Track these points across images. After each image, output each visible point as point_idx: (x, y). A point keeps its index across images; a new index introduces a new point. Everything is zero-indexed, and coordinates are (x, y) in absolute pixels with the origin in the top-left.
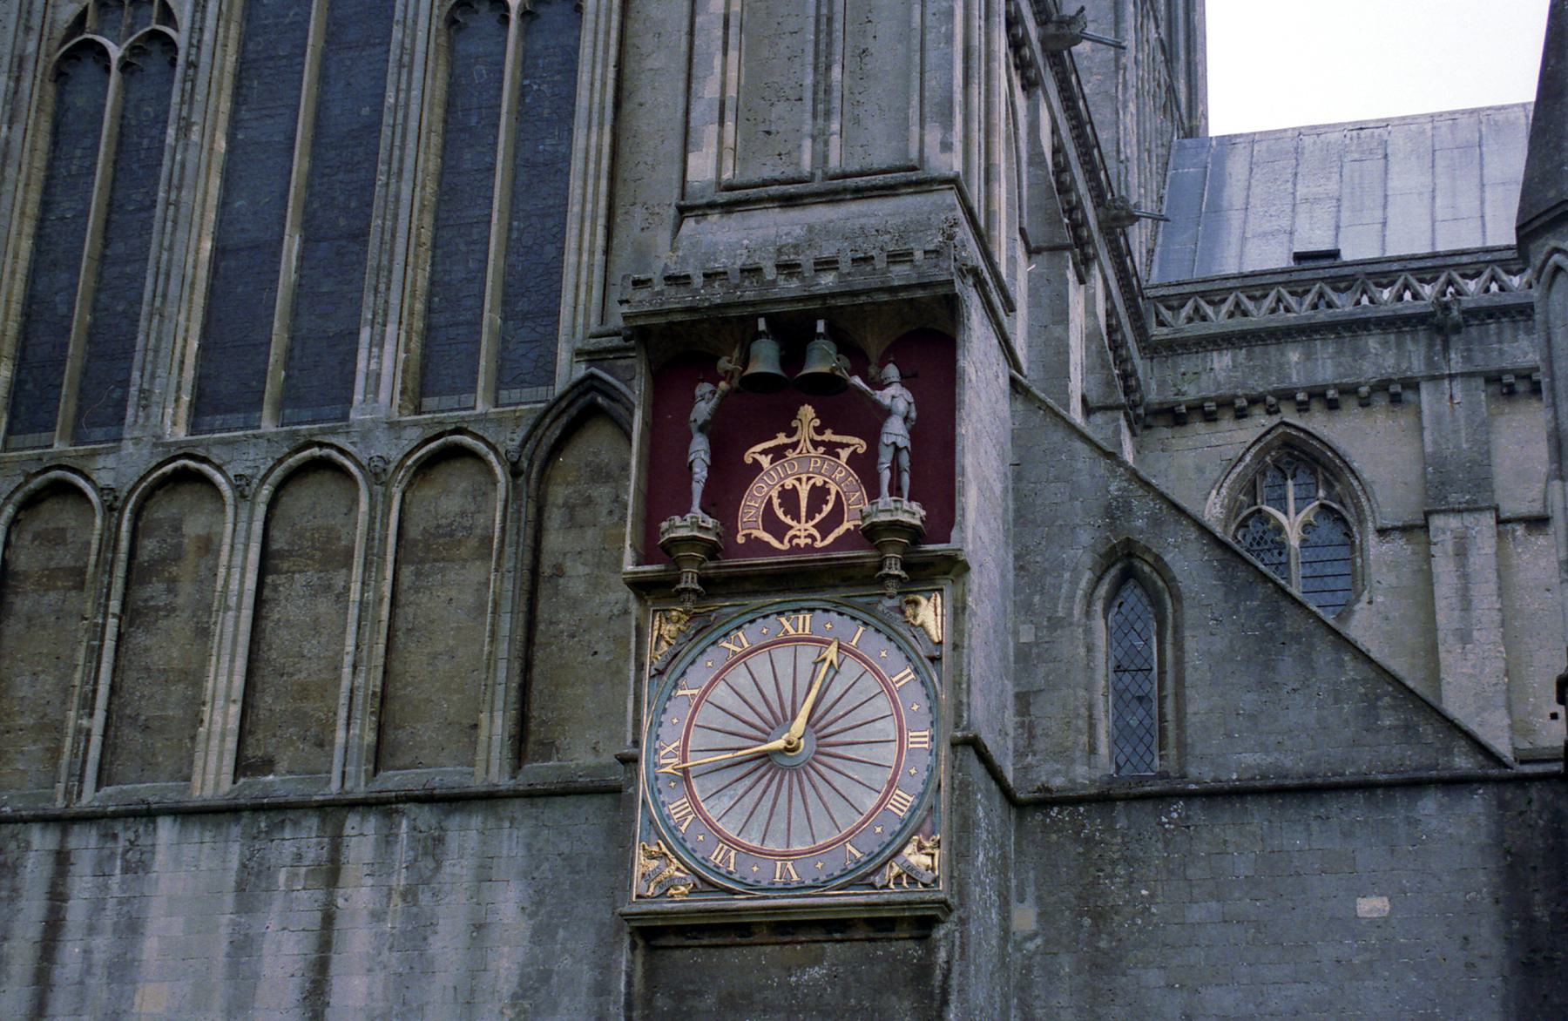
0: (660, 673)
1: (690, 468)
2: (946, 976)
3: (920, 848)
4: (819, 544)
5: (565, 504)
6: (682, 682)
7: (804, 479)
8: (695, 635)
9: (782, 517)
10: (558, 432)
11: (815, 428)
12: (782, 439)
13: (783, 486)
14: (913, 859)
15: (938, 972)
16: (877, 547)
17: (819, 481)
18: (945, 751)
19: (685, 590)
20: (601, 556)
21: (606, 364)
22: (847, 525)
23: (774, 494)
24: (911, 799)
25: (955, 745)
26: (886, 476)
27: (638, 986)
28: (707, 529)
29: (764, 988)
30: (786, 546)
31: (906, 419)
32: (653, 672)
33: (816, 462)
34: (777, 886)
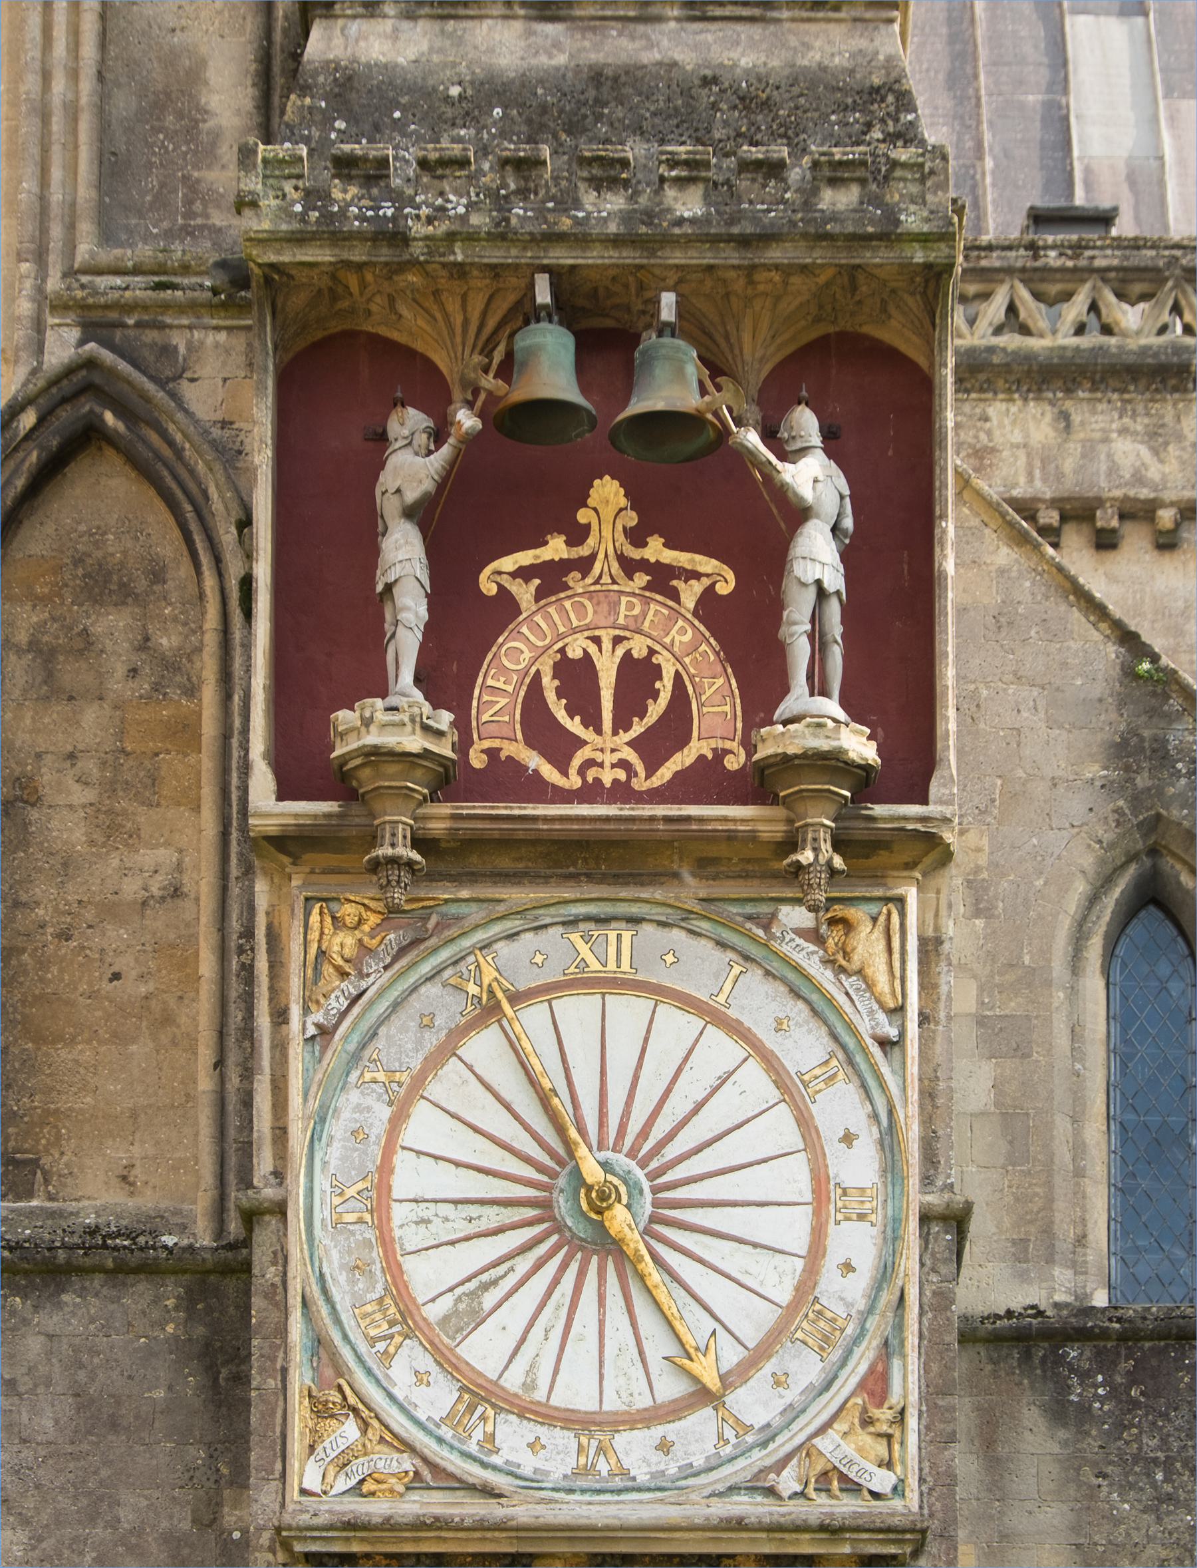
4: (641, 783)
7: (607, 644)
9: (561, 715)
21: (118, 334)
30: (575, 782)
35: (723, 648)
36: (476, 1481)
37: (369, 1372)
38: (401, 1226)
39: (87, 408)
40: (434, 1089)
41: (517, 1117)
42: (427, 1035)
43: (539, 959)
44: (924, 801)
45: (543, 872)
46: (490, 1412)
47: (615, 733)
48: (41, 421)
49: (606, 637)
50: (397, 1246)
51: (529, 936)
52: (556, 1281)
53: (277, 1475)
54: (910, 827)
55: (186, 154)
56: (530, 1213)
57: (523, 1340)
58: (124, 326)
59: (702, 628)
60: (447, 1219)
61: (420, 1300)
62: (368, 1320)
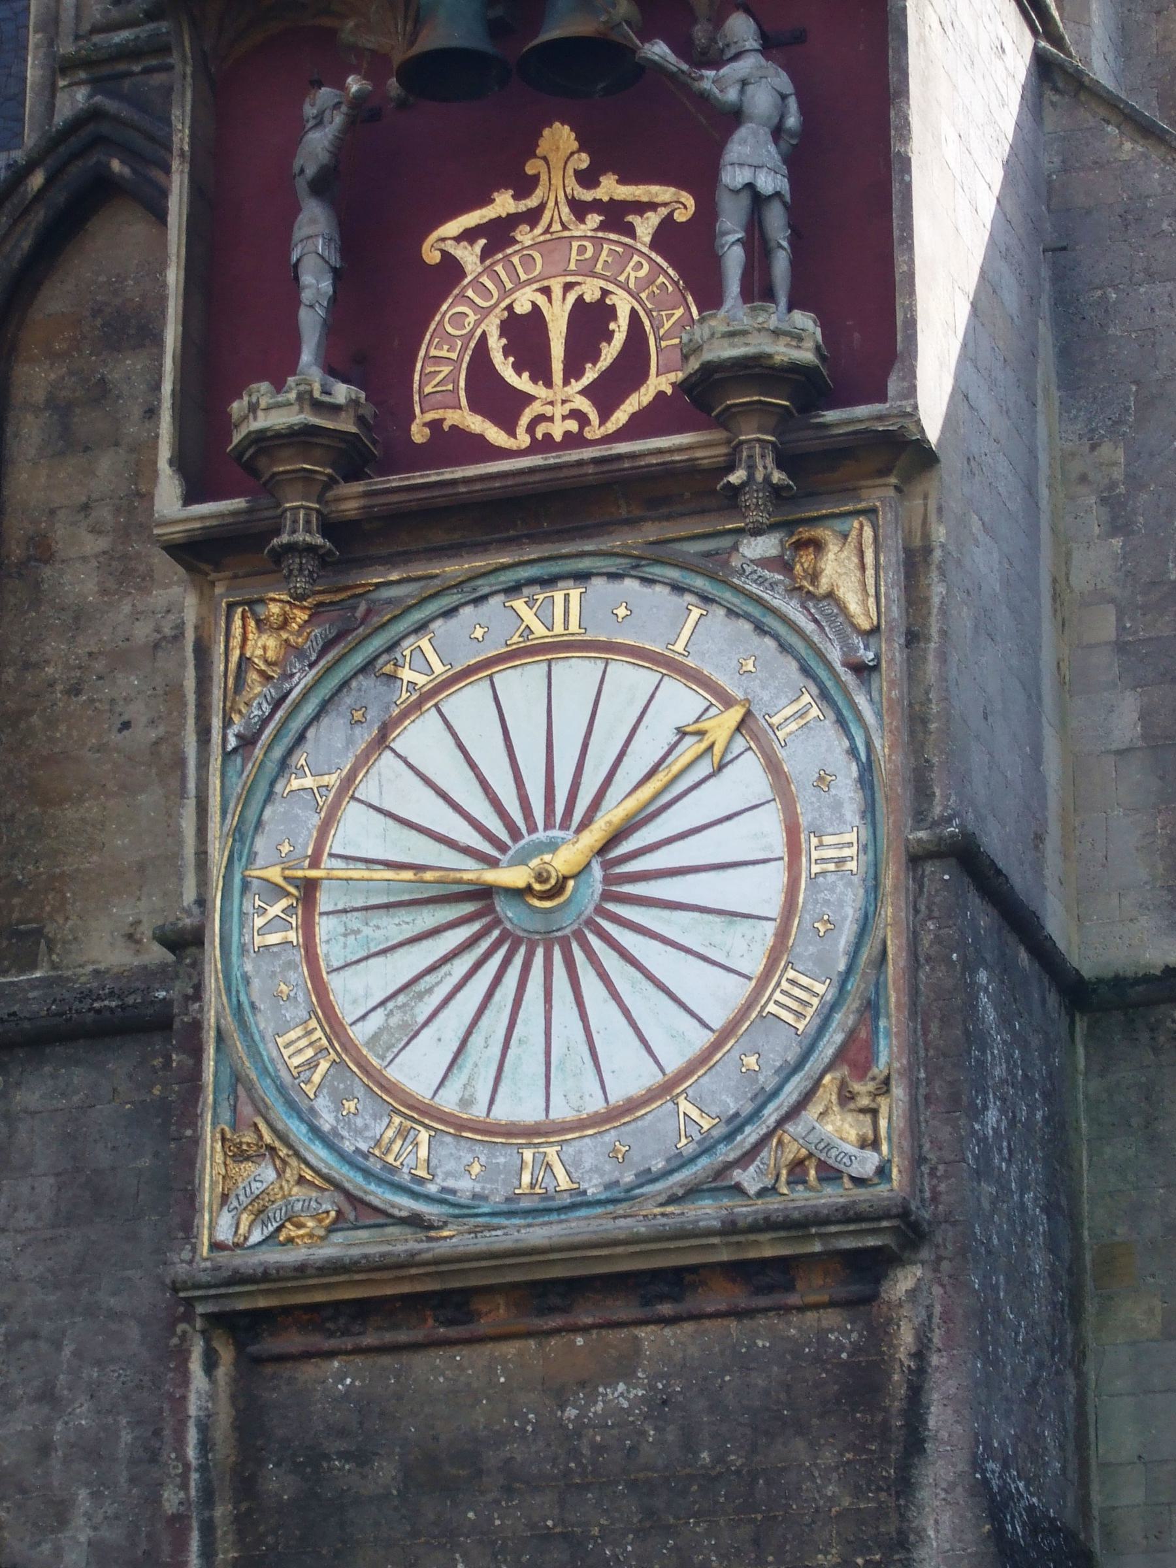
0: (247, 741)
3: (846, 1097)
4: (594, 431)
5: (51, 402)
6: (300, 759)
7: (557, 291)
8: (322, 653)
10: (26, 244)
13: (510, 308)
14: (828, 1128)
15: (896, 1377)
17: (590, 291)
19: (291, 548)
21: (126, 84)
22: (658, 384)
23: (492, 327)
24: (820, 988)
25: (915, 859)
26: (734, 259)
27: (225, 1449)
28: (335, 409)
30: (524, 440)
31: (777, 132)
32: (232, 742)
33: (582, 250)
34: (525, 1204)
35: (681, 276)
36: (404, 1214)
37: (291, 1105)
38: (328, 942)
39: (95, 159)
40: (367, 789)
42: (358, 730)
43: (479, 633)
44: (882, 397)
46: (424, 1136)
47: (566, 382)
48: (49, 181)
50: (322, 964)
51: (467, 611)
56: (468, 908)
58: (131, 74)
59: (659, 260)
61: (348, 1020)
62: (292, 1049)
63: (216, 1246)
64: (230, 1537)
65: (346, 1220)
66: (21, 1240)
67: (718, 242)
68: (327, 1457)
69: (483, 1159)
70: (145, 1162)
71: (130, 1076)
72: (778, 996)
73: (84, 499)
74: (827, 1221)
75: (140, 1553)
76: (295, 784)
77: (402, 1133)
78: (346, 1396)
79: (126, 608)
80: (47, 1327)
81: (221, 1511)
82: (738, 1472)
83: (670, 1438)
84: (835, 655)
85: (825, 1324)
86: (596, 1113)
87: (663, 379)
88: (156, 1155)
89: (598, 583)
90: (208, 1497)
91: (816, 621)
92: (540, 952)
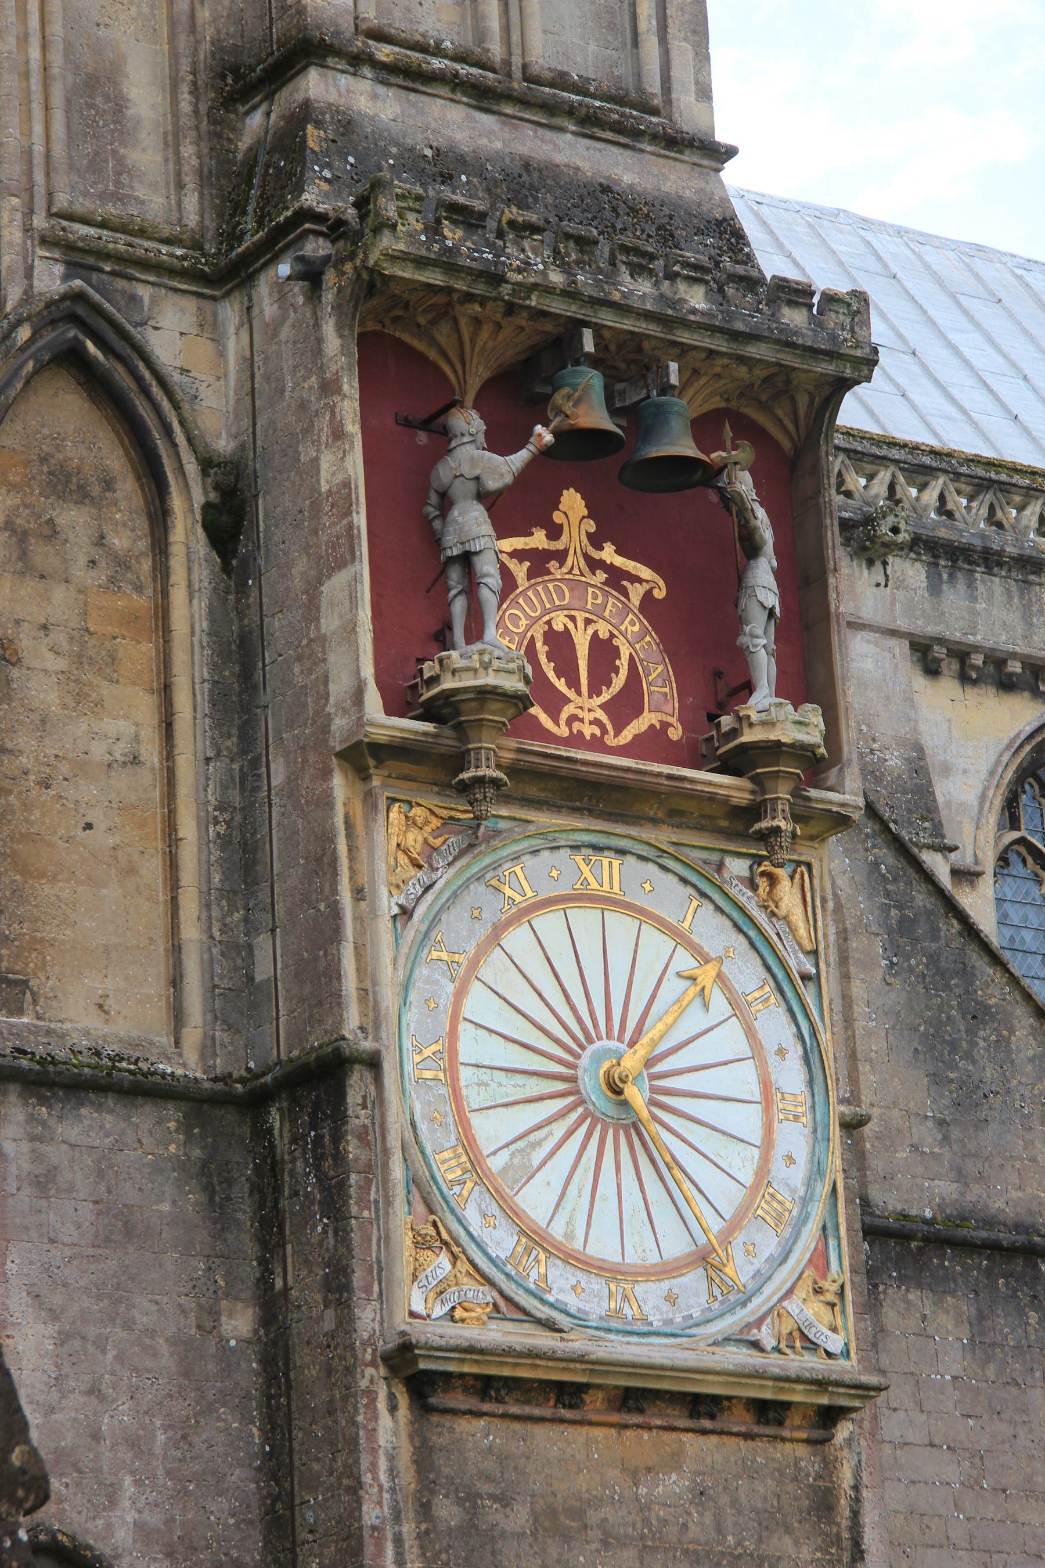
0: (406, 913)
1: (467, 559)
2: (855, 1514)
3: (818, 1291)
7: (581, 624)
11: (588, 534)
12: (538, 540)
13: (549, 623)
14: (809, 1313)
15: (843, 1502)
16: (754, 779)
18: (836, 1132)
20: (83, 644)
21: (95, 276)
24: (789, 1206)
27: (408, 1477)
29: (598, 1502)
30: (563, 731)
32: (396, 910)
36: (543, 1316)
38: (467, 1087)
41: (547, 1004)
42: (477, 925)
45: (559, 802)
46: (542, 1256)
47: (590, 697)
49: (580, 616)
51: (546, 854)
52: (584, 1147)
53: (375, 1296)
54: (835, 809)
55: (113, 131)
56: (561, 1086)
57: (563, 1194)
58: (101, 270)
60: (501, 1085)
61: (485, 1153)
62: (446, 1166)
63: (412, 1314)
64: (415, 1550)
65: (499, 1312)
66: (68, 1252)
67: (743, 640)
68: (480, 1496)
69: (583, 1285)
70: (166, 1207)
71: (150, 1132)
72: (763, 1204)
73: (43, 621)
74: (838, 1384)
75: (176, 1538)
76: (435, 955)
77: (528, 1251)
78: (490, 1449)
79: (84, 727)
80: (92, 1331)
81: (408, 1529)
82: (751, 1555)
83: (707, 1522)
84: (792, 963)
85: (798, 1454)
86: (656, 1265)
87: (653, 715)
88: (174, 1202)
89: (630, 860)
90: (397, 1517)
91: (778, 934)
92: (611, 1132)
